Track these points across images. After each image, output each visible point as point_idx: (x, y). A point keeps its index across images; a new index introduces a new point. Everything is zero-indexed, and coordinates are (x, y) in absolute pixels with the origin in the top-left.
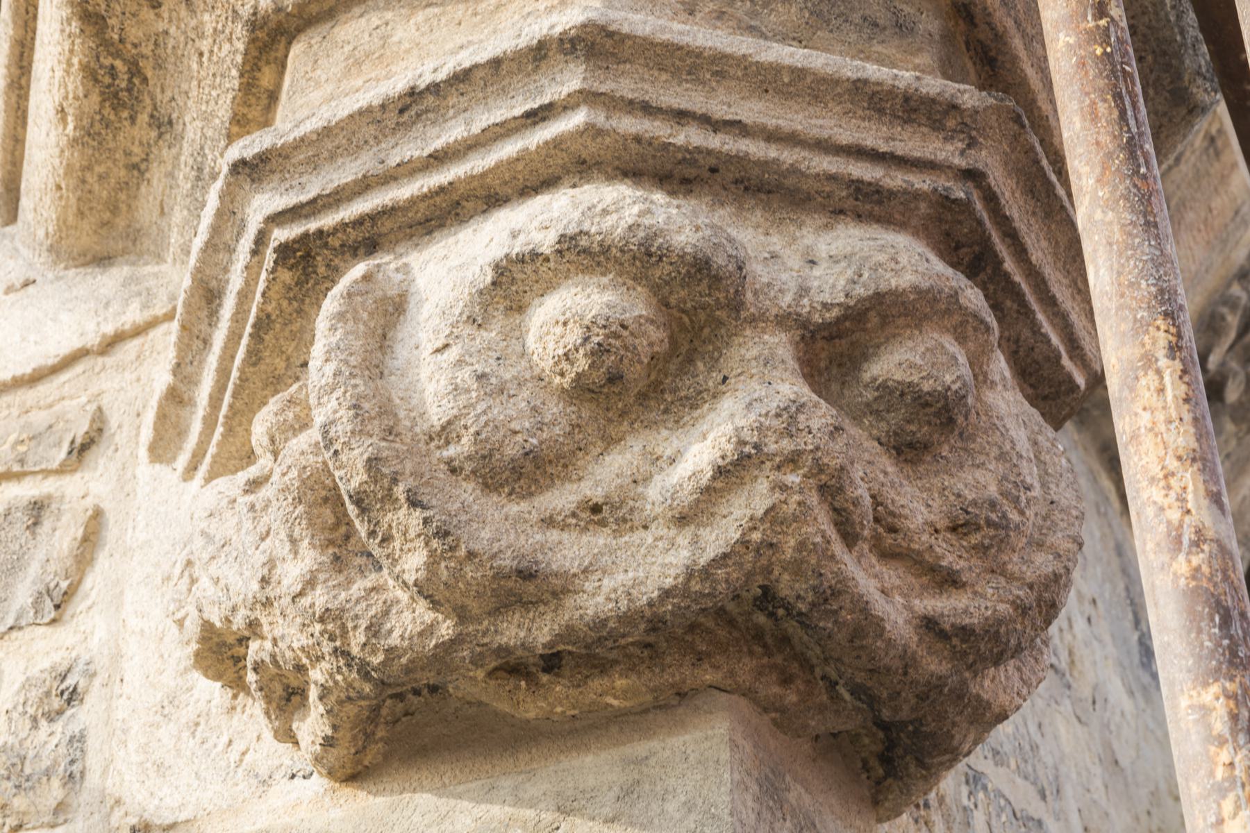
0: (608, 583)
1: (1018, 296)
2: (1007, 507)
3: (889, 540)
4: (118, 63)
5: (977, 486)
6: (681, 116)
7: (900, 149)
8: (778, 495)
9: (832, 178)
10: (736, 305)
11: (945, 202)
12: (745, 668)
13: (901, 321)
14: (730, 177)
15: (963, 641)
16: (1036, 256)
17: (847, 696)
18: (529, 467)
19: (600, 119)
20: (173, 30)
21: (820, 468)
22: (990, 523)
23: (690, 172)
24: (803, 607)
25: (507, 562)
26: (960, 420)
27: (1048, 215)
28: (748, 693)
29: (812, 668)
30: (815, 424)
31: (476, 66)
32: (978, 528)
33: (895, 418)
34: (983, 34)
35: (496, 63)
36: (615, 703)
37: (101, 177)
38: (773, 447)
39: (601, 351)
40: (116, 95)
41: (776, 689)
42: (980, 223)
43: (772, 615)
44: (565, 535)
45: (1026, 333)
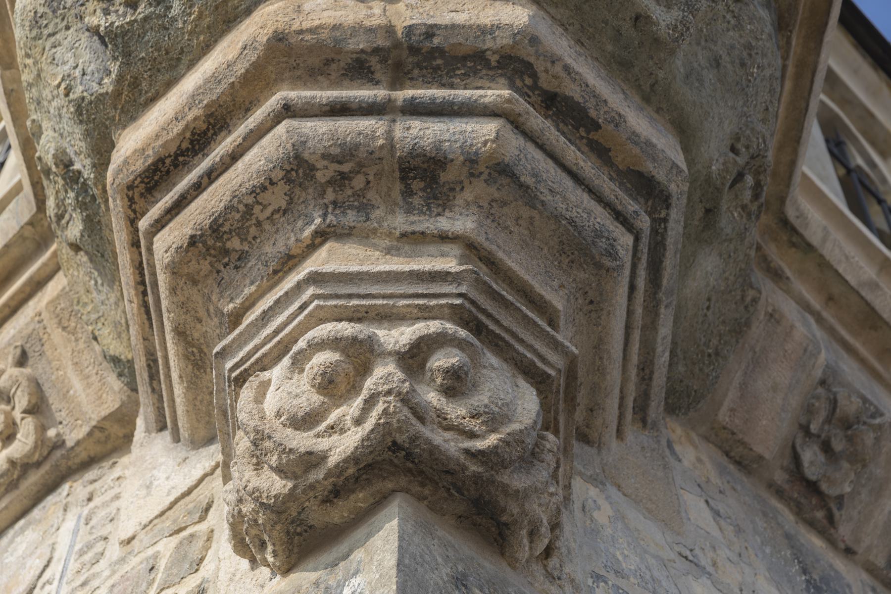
0: (337, 451)
1: (503, 339)
2: (493, 406)
3: (445, 423)
4: (194, 349)
5: (479, 401)
6: (350, 296)
7: (431, 291)
8: (386, 405)
9: (409, 306)
10: (372, 351)
11: (452, 306)
12: (403, 481)
13: (434, 346)
14: (373, 314)
15: (483, 456)
16: (505, 323)
17: (456, 494)
18: (308, 419)
19: (322, 303)
20: (208, 330)
21: (400, 393)
22: (486, 413)
23: (360, 315)
24: (407, 445)
25: (302, 450)
26: (463, 376)
27: (507, 307)
28: (407, 491)
29: (437, 484)
30: (396, 379)
31: (280, 297)
32: (482, 415)
33: (439, 381)
34: (485, 253)
35: (286, 293)
36: (362, 505)
37: (201, 402)
38: (380, 389)
39: (324, 373)
40: (197, 364)
41: (418, 489)
42: (471, 312)
43: (413, 462)
44: (324, 440)
45: (515, 355)
